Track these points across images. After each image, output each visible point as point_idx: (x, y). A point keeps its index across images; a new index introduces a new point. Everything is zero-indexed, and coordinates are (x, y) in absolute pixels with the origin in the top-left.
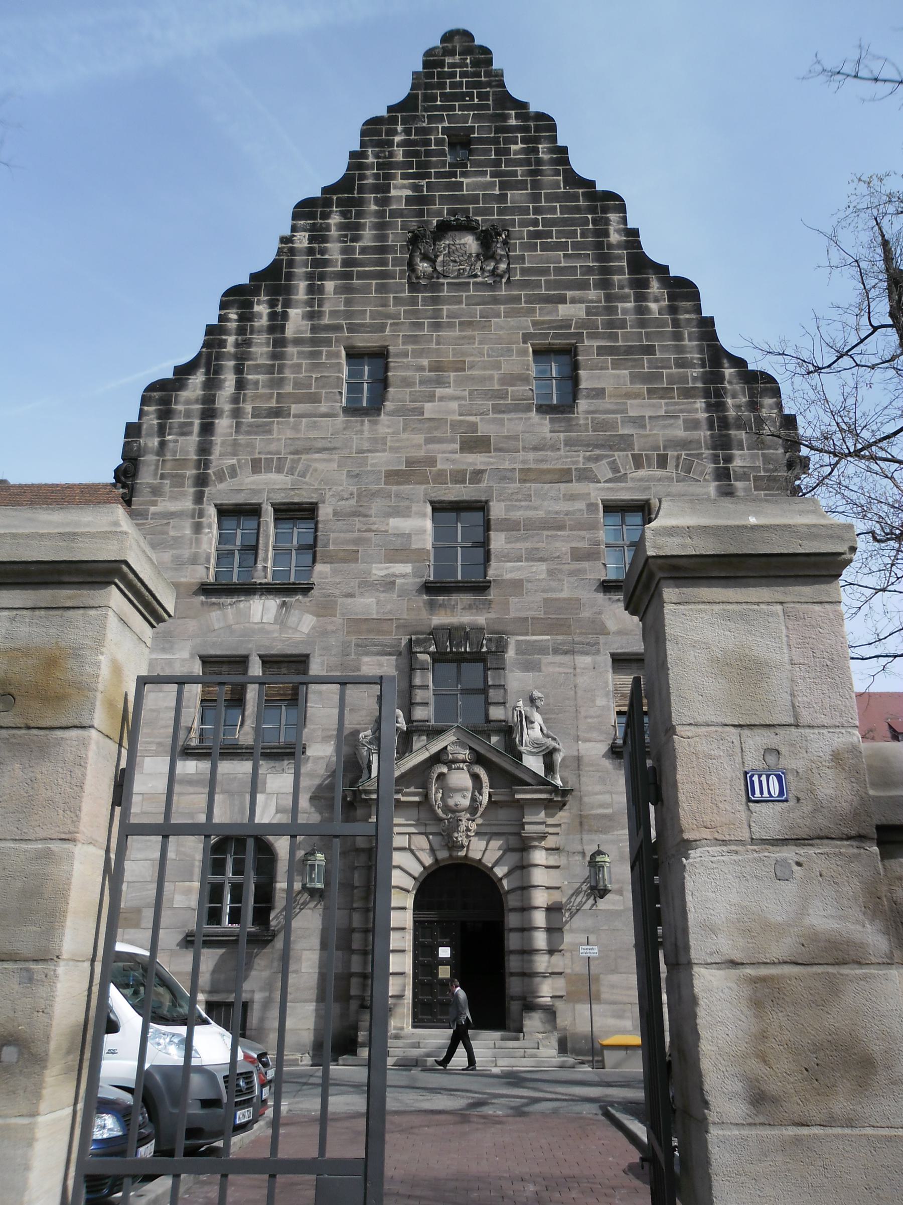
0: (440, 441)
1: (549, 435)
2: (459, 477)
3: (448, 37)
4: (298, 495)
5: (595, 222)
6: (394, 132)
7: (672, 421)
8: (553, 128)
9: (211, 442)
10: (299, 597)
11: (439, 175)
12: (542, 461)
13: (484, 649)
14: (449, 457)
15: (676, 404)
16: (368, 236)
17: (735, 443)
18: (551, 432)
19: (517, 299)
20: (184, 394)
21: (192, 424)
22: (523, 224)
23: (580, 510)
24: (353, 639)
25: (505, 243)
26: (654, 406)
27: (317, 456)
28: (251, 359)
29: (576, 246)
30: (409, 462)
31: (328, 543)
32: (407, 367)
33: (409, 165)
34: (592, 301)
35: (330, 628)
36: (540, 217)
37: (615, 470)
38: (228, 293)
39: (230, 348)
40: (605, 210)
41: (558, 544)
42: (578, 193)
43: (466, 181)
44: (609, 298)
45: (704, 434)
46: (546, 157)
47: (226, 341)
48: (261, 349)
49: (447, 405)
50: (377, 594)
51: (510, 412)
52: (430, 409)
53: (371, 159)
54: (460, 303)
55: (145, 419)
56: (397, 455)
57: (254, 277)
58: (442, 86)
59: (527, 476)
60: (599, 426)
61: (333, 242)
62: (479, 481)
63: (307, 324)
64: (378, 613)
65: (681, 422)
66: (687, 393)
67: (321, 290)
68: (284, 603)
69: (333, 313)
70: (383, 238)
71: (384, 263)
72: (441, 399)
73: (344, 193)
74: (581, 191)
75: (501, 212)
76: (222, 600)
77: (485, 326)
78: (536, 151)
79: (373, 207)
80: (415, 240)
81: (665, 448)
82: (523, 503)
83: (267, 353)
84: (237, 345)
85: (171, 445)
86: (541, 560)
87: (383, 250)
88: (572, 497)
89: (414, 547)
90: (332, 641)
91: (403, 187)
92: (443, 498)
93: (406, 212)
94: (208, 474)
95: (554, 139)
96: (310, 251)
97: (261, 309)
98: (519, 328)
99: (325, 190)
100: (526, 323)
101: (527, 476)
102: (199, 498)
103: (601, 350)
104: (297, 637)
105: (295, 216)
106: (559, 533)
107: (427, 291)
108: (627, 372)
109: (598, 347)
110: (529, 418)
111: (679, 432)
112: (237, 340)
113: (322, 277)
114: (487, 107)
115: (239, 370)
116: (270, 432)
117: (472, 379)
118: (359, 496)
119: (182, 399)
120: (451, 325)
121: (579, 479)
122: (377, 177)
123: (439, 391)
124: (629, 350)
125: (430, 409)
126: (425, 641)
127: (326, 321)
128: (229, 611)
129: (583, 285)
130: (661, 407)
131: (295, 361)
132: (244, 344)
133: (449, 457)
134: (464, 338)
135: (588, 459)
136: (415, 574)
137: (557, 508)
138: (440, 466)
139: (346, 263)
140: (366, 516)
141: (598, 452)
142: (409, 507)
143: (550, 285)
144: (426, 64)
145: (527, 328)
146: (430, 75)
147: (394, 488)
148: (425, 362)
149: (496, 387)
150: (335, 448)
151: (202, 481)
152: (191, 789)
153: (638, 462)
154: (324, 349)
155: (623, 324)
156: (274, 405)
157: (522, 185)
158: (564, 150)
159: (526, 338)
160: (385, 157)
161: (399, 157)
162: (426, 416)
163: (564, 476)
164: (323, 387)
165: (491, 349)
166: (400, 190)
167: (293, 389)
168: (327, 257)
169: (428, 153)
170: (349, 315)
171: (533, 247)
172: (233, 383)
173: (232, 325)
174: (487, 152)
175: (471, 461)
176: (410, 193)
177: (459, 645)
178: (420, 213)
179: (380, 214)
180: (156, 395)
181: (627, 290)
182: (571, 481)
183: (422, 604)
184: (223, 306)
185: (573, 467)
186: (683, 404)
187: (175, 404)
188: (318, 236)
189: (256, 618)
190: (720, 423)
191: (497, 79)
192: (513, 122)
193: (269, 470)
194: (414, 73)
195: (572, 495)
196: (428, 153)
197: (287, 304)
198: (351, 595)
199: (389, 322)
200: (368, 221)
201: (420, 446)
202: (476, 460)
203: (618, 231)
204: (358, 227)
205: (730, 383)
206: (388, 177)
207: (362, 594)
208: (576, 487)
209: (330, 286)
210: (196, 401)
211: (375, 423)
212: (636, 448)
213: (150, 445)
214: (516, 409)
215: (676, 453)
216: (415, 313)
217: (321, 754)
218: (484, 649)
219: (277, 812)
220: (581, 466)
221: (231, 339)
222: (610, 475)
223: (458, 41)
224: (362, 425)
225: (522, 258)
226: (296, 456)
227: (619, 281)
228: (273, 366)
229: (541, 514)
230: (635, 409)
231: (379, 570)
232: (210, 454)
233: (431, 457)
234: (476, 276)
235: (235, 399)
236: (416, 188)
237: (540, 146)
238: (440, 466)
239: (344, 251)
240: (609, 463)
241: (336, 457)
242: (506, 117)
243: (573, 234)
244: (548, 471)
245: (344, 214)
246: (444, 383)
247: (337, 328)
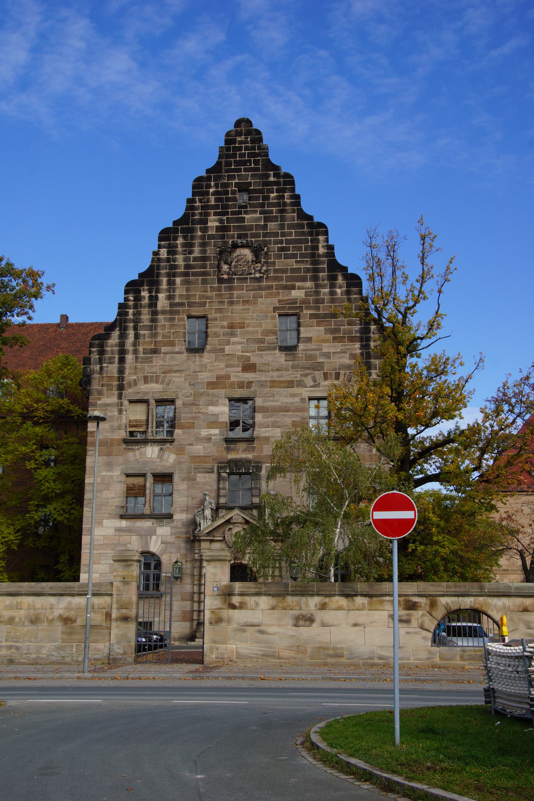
0: (232, 366)
1: (284, 363)
2: (241, 385)
3: (238, 123)
4: (167, 395)
5: (312, 241)
6: (209, 187)
7: (343, 355)
8: (292, 183)
9: (124, 367)
10: (168, 445)
11: (233, 213)
12: (280, 376)
13: (251, 471)
14: (237, 375)
15: (347, 345)
16: (197, 252)
17: (373, 366)
18: (285, 361)
19: (270, 287)
20: (110, 342)
21: (114, 358)
22: (276, 242)
23: (297, 402)
24: (193, 465)
25: (266, 253)
26: (335, 346)
27: (174, 374)
28: (141, 322)
29: (302, 256)
30: (218, 378)
31: (181, 419)
32: (217, 326)
33: (217, 207)
34: (308, 288)
35: (182, 460)
36: (284, 239)
37: (315, 380)
38: (128, 285)
39: (131, 316)
40: (318, 234)
41: (286, 419)
42: (304, 223)
43: (247, 216)
44: (317, 286)
46: (288, 201)
47: (128, 312)
48: (145, 317)
49: (236, 347)
50: (203, 444)
51: (266, 350)
52: (228, 349)
53: (198, 204)
54: (243, 290)
55: (92, 355)
56: (213, 374)
57: (140, 275)
58: (234, 156)
59: (273, 384)
60: (309, 357)
61: (179, 254)
62: (250, 387)
63: (167, 303)
64: (204, 453)
65: (347, 355)
66: (352, 339)
67: (174, 283)
68: (161, 449)
69: (181, 296)
70: (204, 252)
71: (204, 267)
72: (233, 344)
73: (184, 225)
74: (306, 222)
75: (265, 235)
76: (133, 447)
77: (255, 303)
78: (283, 197)
79: (199, 233)
80: (221, 253)
81: (339, 369)
82: (271, 399)
83: (149, 319)
84: (134, 314)
85: (105, 369)
86: (278, 427)
87: (204, 259)
88: (293, 395)
89: (220, 420)
90: (184, 466)
91: (215, 221)
92: (233, 396)
93: (216, 236)
94: (124, 384)
95: (293, 190)
96: (168, 260)
97: (145, 294)
98: (271, 304)
99: (175, 223)
100: (274, 301)
101: (273, 384)
102: (120, 396)
103: (312, 316)
104: (168, 464)
105: (160, 239)
106: (287, 413)
107: (227, 283)
108: (323, 328)
109: (310, 314)
110: (275, 354)
111: (346, 361)
112: (134, 311)
113: (175, 275)
114: (258, 169)
115: (135, 328)
116: (152, 362)
117: (248, 332)
118: (195, 395)
119: (109, 344)
120: (238, 302)
121: (298, 386)
122: (201, 214)
123: (233, 340)
124: (325, 316)
125: (228, 349)
126: (225, 467)
127: (177, 300)
128: (137, 452)
129: (304, 279)
130: (338, 347)
131: (163, 323)
132: (137, 314)
133: (237, 375)
134: (244, 310)
135: (302, 375)
136: (221, 434)
137: (286, 401)
138: (232, 379)
139: (187, 267)
140: (198, 405)
141: (307, 371)
142: (217, 401)
143: (288, 279)
144: (227, 142)
145: (275, 304)
146: (228, 149)
147: (211, 391)
148: (225, 324)
149: (260, 337)
150: (183, 370)
151: (121, 388)
152: (124, 534)
153: (326, 376)
154: (176, 316)
155: (323, 301)
156: (153, 347)
157: (275, 219)
158: (298, 197)
159: (275, 309)
160: (205, 202)
161: (213, 203)
162: (226, 353)
163: (290, 384)
164: (176, 338)
165: (258, 316)
166: (213, 223)
167: (162, 338)
168: (176, 263)
169: (228, 199)
170: (188, 297)
171: (279, 257)
172: (133, 335)
173: (131, 303)
174: (258, 198)
175: (246, 376)
176: (218, 224)
177: (239, 469)
178: (223, 237)
179: (203, 237)
180: (97, 342)
181: (326, 282)
182: (293, 387)
183: (223, 449)
184: (126, 292)
185: (295, 379)
186: (350, 345)
187: (106, 347)
188: (172, 251)
189: (149, 456)
191: (264, 151)
192: (272, 179)
193: (152, 382)
194: (220, 147)
195: (294, 394)
196: (228, 199)
197: (158, 291)
198: (191, 445)
199: (208, 301)
200: (197, 242)
201: (223, 369)
202: (249, 376)
203: (323, 247)
204: (192, 245)
205: (373, 333)
207: (196, 444)
208: (296, 390)
209: (178, 280)
210: (116, 346)
211: (201, 357)
212: (325, 369)
213: (95, 369)
214: (268, 349)
215: (344, 372)
216: (220, 295)
217: (180, 518)
218: (251, 471)
219: (162, 543)
220: (299, 379)
221: (131, 311)
222: (312, 384)
223: (244, 125)
224: (195, 358)
225: (274, 263)
226: (164, 375)
227: (323, 276)
228: (152, 326)
229: (279, 404)
230: (327, 348)
231: (204, 432)
232: (124, 374)
233: (228, 375)
234: (251, 274)
235: (135, 344)
236: (221, 221)
237: (286, 194)
238: (232, 379)
239: (186, 260)
240: (312, 378)
241: (183, 375)
242: (268, 176)
243: (300, 249)
244: (283, 382)
245: (185, 238)
246: (235, 335)
247: (182, 304)
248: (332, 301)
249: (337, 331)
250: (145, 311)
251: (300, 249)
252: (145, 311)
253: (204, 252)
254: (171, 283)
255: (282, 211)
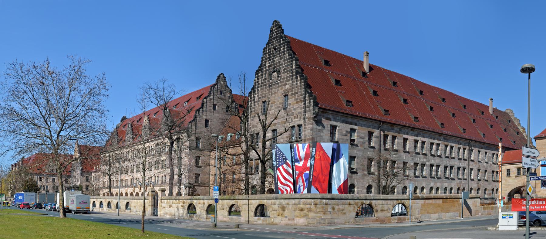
19: (281, 86)
44: (293, 82)
45: (303, 110)
48: (253, 104)
66: (301, 102)
75: (280, 65)
96: (258, 82)
97: (253, 96)
103: (292, 94)
111: (300, 110)
139: (262, 83)
166: (267, 65)
170: (262, 94)
171: (283, 73)
190: (305, 107)
200: (264, 73)
206: (266, 62)
236: (269, 63)
248: (297, 87)
249: (297, 99)
250: (253, 102)
251: (288, 68)
252: (253, 102)
253: (265, 76)
254: (258, 90)
255: (284, 54)
